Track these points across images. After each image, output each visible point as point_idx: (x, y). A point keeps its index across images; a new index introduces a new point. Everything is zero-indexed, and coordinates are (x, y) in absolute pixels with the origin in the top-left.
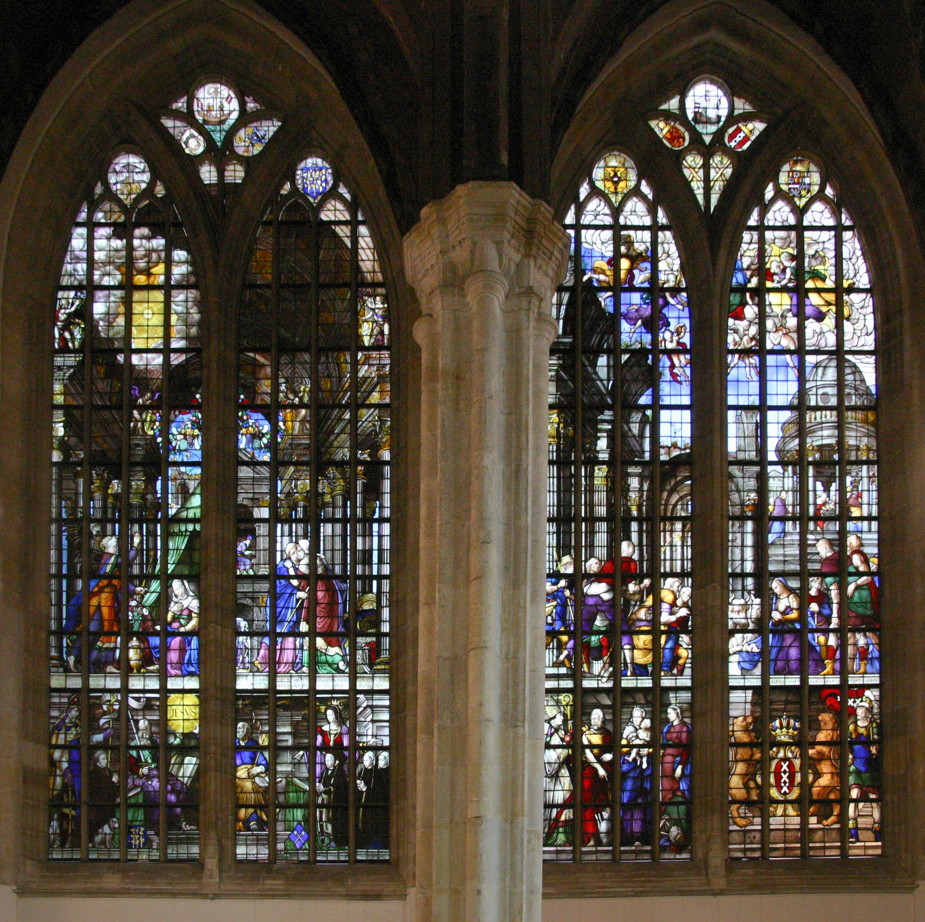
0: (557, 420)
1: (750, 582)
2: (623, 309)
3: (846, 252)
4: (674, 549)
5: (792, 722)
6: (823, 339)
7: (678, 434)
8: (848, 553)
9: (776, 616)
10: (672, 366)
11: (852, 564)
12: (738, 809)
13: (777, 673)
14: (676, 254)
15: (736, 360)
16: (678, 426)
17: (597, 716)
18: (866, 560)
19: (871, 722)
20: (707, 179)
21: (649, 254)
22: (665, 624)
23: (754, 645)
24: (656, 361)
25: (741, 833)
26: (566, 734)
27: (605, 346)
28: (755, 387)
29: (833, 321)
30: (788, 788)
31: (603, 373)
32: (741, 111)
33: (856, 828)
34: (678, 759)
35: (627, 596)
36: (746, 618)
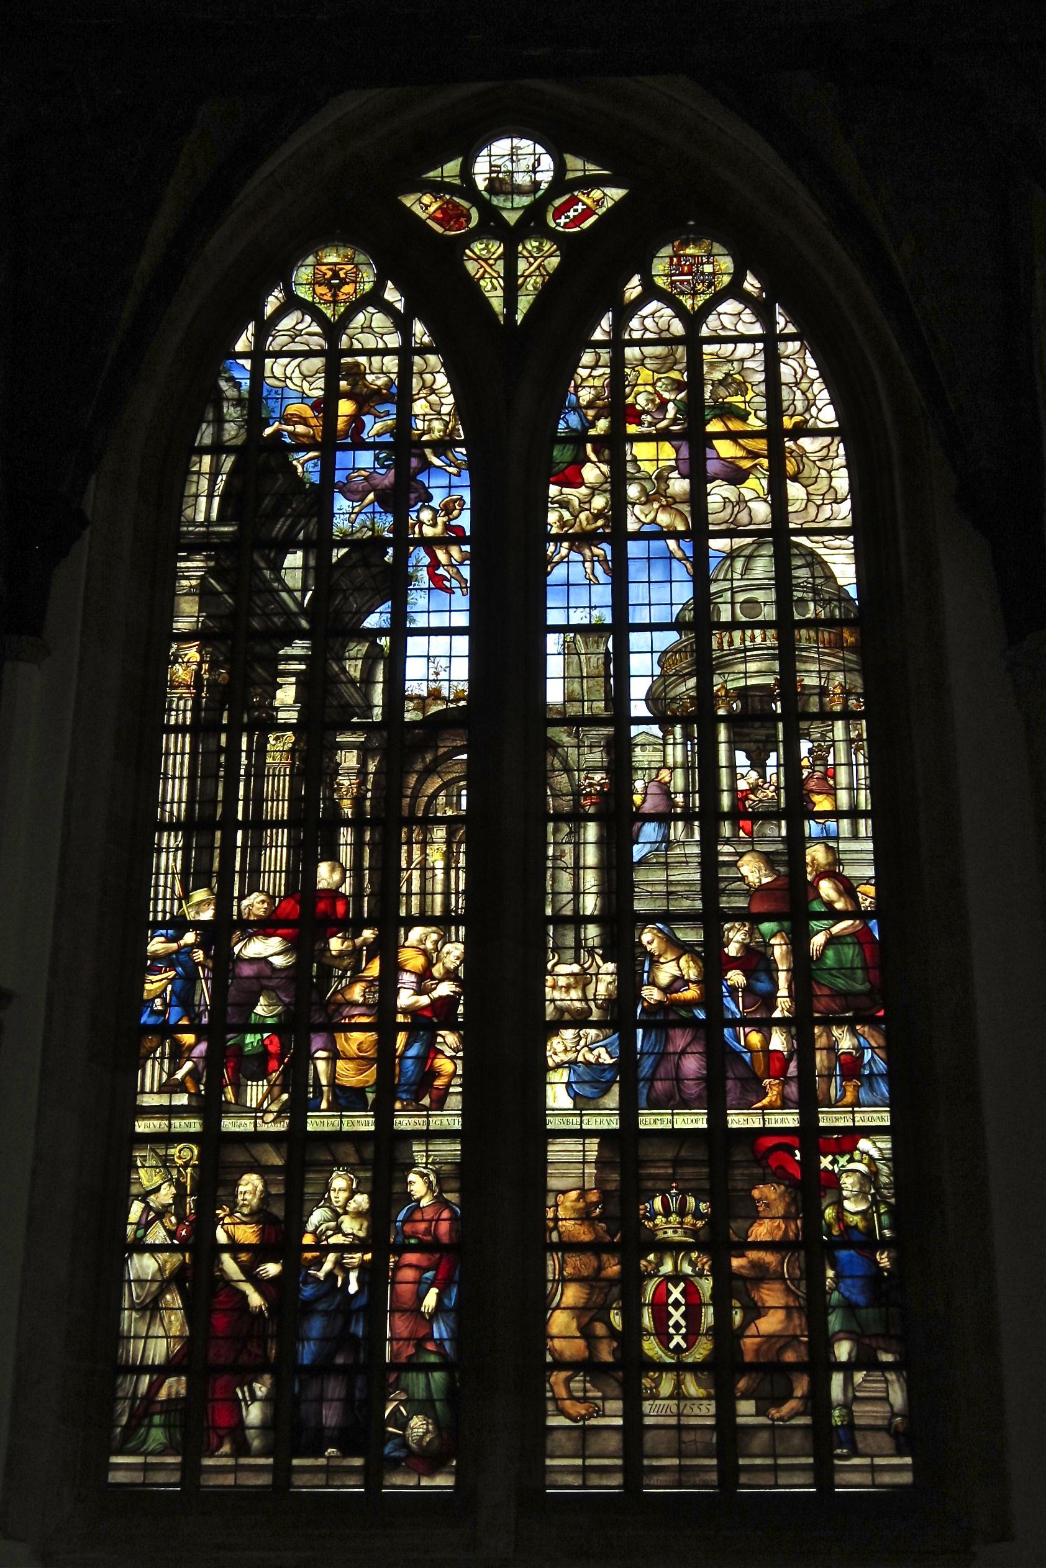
5: (691, 1201)
12: (567, 1381)
13: (655, 1104)
17: (249, 1188)
23: (602, 1050)
30: (684, 1337)
34: (429, 1274)
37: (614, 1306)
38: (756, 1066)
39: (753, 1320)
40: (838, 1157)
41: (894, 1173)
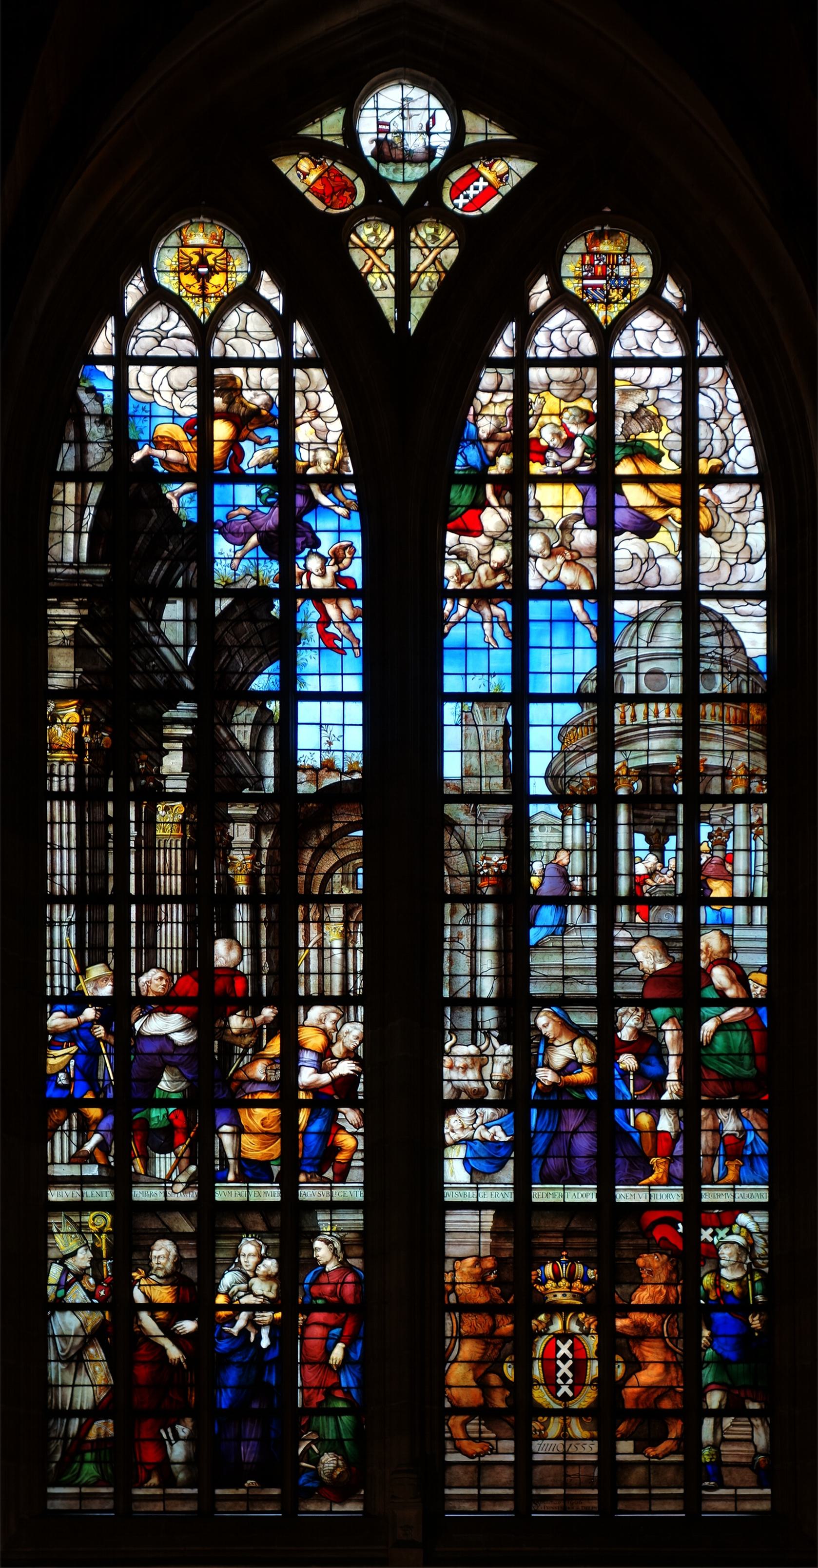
0: (77, 718)
1: (489, 1016)
2: (219, 514)
3: (705, 405)
4: (327, 953)
6: (655, 570)
7: (337, 745)
8: (703, 965)
9: (546, 1076)
10: (325, 621)
11: (711, 983)
12: (465, 1424)
14: (334, 412)
15: (462, 610)
16: (337, 731)
17: (162, 1252)
18: (740, 977)
19: (750, 1272)
20: (402, 271)
21: (275, 412)
22: (307, 1089)
24: (290, 611)
25: (471, 1469)
26: (98, 1282)
27: (180, 583)
28: (503, 660)
29: (676, 537)
30: (571, 1387)
31: (174, 633)
32: (481, 138)
33: (718, 1463)
34: (336, 1331)
35: (228, 1039)
36: (482, 1080)
37: (507, 1359)
38: (644, 1145)
39: (634, 1373)
40: (718, 1230)
41: (769, 1245)
